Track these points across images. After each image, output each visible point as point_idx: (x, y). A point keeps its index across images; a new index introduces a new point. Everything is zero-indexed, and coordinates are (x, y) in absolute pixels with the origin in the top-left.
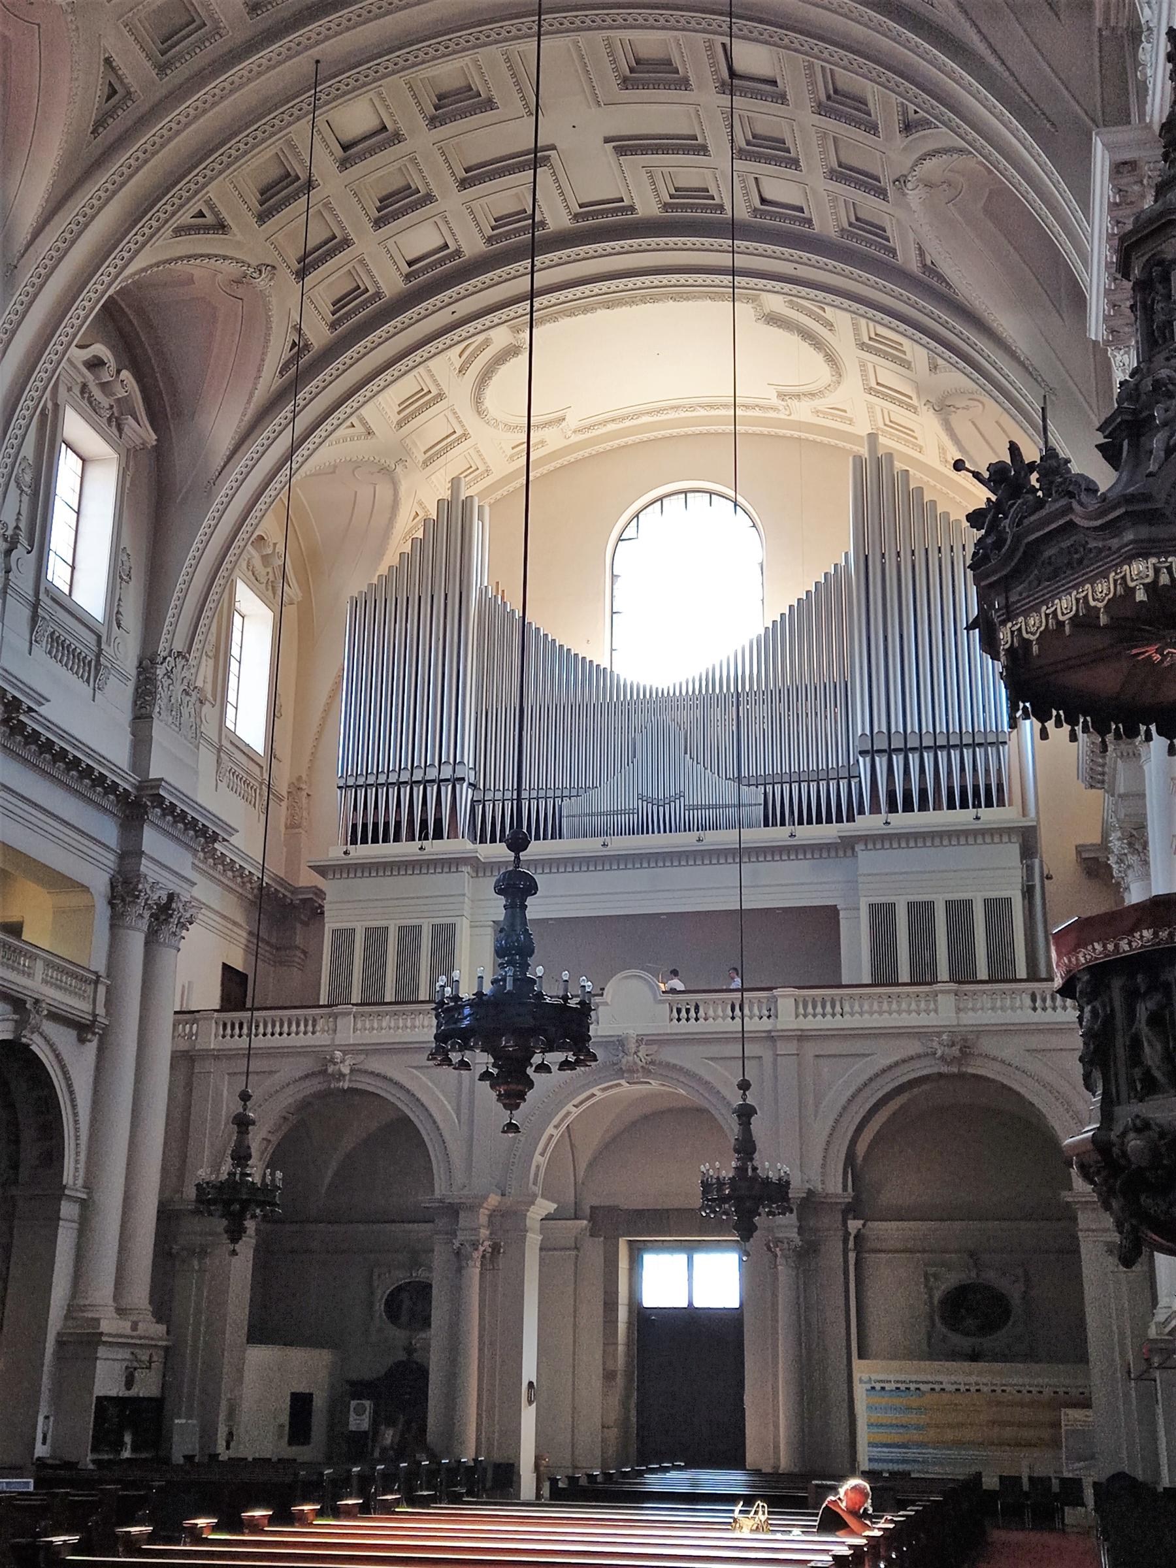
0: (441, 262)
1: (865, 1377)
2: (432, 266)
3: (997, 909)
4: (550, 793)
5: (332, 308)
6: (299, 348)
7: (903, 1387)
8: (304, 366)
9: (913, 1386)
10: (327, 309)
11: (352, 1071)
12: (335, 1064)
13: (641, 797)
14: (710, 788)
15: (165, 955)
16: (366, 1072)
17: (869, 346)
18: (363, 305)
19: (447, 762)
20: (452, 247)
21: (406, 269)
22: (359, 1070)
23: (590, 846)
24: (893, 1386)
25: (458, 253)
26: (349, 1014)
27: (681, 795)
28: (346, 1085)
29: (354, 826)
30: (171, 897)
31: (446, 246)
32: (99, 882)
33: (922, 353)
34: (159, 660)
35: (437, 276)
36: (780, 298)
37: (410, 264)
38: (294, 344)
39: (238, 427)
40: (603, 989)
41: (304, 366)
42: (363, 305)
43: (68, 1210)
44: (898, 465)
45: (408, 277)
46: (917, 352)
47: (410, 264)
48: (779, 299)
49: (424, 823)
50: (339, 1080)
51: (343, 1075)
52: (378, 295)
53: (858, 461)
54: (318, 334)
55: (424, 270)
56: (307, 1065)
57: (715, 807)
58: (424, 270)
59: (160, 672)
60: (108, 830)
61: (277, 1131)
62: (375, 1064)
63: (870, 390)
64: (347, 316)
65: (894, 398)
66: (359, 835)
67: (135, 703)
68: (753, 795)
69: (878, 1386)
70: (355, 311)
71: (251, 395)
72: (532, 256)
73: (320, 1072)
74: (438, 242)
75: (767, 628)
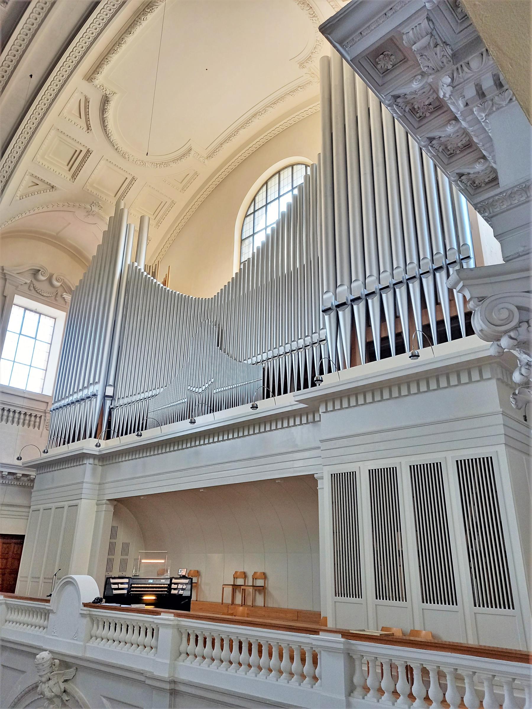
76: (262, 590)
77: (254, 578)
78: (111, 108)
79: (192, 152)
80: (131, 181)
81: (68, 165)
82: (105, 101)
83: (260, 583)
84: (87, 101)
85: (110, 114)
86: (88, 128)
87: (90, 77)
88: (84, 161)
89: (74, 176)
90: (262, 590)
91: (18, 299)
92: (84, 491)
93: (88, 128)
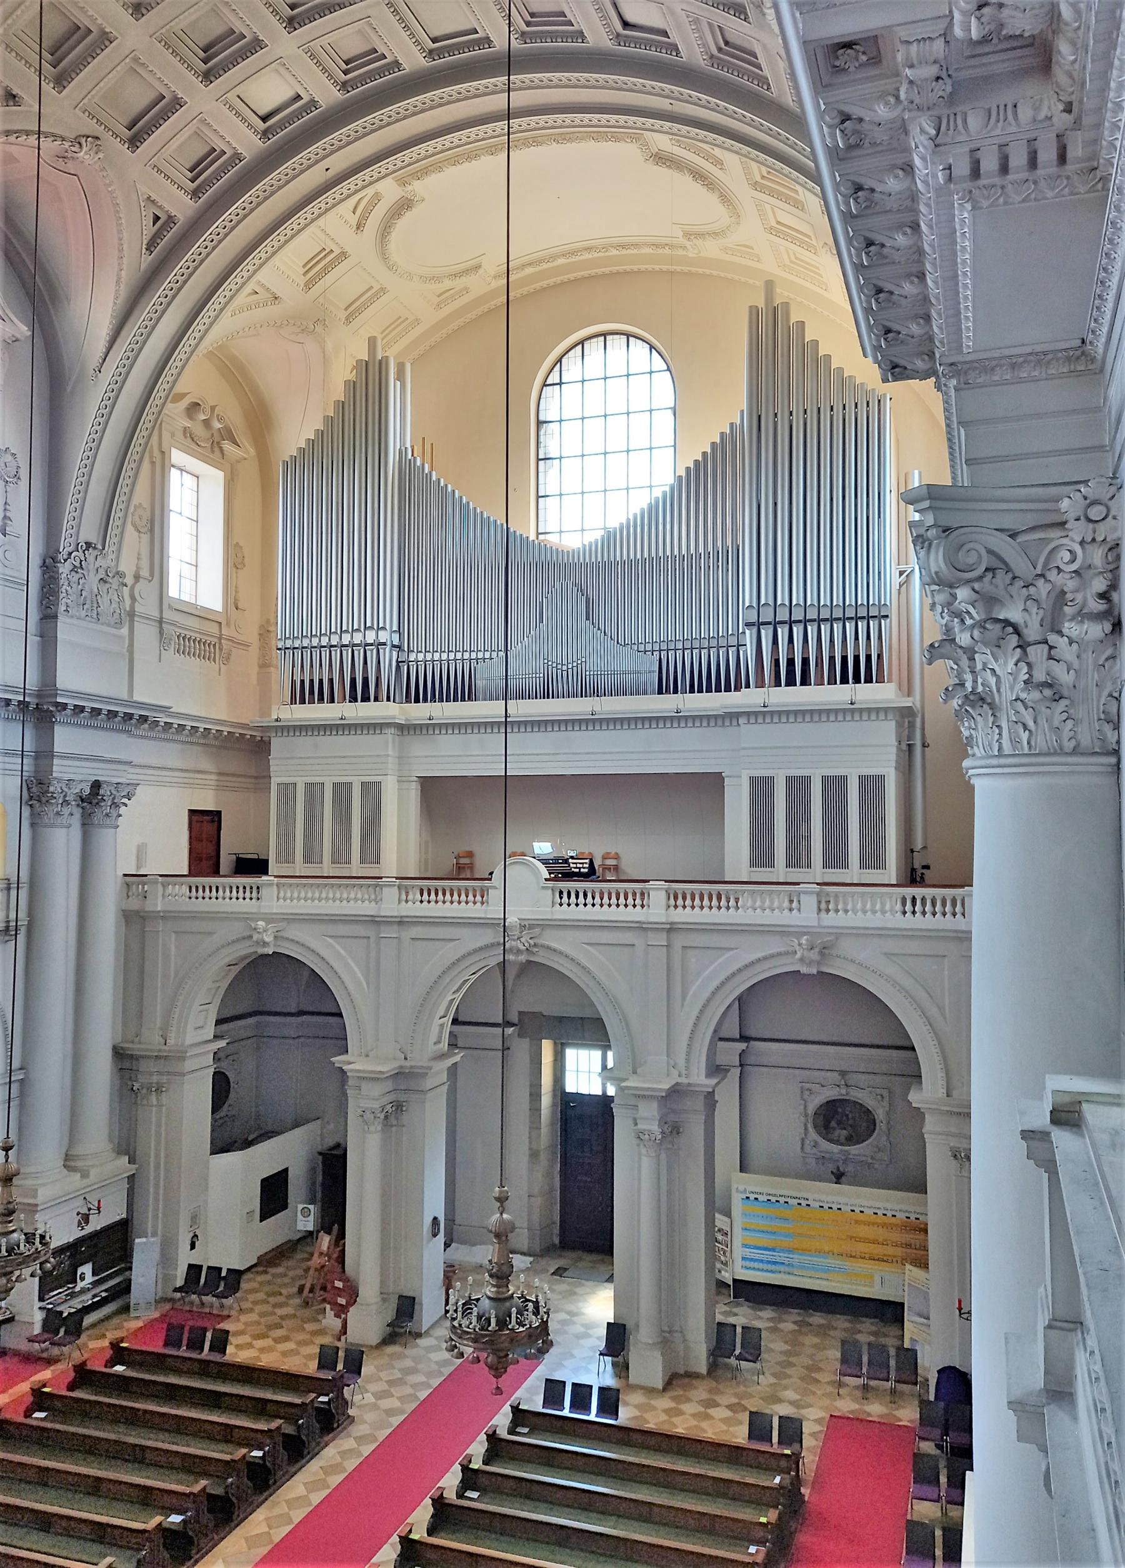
0: (297, 115)
1: (741, 1188)
2: (289, 120)
3: (872, 786)
5: (190, 175)
6: (162, 222)
7: (773, 1199)
8: (169, 243)
9: (782, 1200)
11: (275, 937)
15: (104, 836)
16: (287, 939)
17: (763, 186)
18: (224, 170)
22: (282, 937)
24: (765, 1198)
25: (313, 103)
26: (272, 884)
30: (96, 785)
31: (298, 97)
34: (60, 557)
35: (294, 132)
36: (666, 137)
37: (264, 119)
38: (157, 218)
39: (113, 311)
40: (491, 874)
41: (169, 243)
42: (224, 170)
44: (794, 318)
45: (265, 134)
47: (264, 119)
48: (665, 138)
52: (237, 157)
53: (754, 312)
55: (281, 125)
58: (281, 125)
61: (224, 978)
62: (293, 932)
63: (771, 230)
64: (208, 183)
65: (794, 238)
69: (752, 1196)
74: (289, 94)
75: (680, 477)
76: (616, 868)
77: (604, 858)
78: (408, 216)
79: (481, 271)
80: (376, 293)
81: (304, 266)
82: (405, 205)
83: (610, 862)
84: (377, 197)
86: (359, 227)
88: (333, 265)
89: (308, 286)
90: (616, 868)
91: (177, 456)
92: (390, 766)
93: (359, 227)
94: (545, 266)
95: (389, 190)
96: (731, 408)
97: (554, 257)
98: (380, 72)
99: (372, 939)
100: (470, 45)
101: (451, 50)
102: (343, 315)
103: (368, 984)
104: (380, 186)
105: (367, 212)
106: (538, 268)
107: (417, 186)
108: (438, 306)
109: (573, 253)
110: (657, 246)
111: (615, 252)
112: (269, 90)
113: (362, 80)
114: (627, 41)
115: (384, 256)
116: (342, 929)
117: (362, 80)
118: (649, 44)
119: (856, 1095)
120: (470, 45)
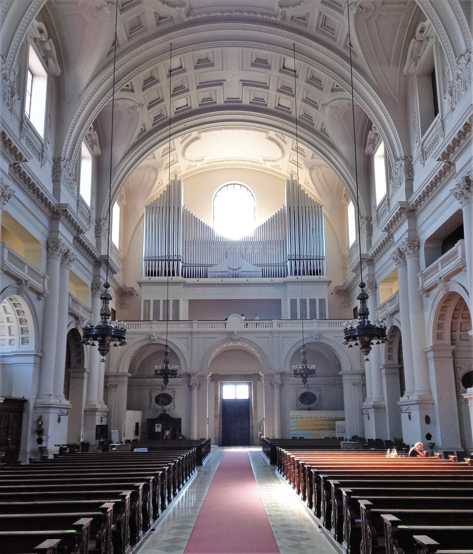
0: (185, 110)
2: (183, 111)
4: (192, 265)
6: (143, 130)
8: (145, 135)
10: (153, 119)
12: (153, 336)
13: (229, 268)
14: (247, 266)
16: (161, 339)
18: (162, 120)
19: (176, 255)
20: (189, 105)
21: (175, 111)
23: (218, 280)
25: (190, 108)
27: (240, 268)
28: (155, 342)
29: (149, 271)
31: (187, 105)
32: (89, 283)
33: (311, 152)
35: (185, 114)
37: (177, 109)
41: (145, 135)
42: (162, 120)
43: (86, 375)
46: (308, 151)
49: (169, 272)
50: (154, 341)
51: (155, 339)
54: (149, 127)
56: (144, 337)
57: (249, 272)
59: (102, 223)
60: (90, 268)
66: (150, 274)
67: (95, 232)
68: (259, 269)
70: (160, 121)
71: (129, 143)
72: (211, 111)
73: (148, 339)
78: (197, 142)
84: (190, 135)
85: (193, 144)
87: (200, 133)
94: (220, 163)
95: (194, 134)
96: (281, 202)
97: (223, 161)
98: (210, 103)
99: (189, 338)
100: (236, 102)
101: (230, 102)
102: (165, 166)
103: (188, 351)
104: (193, 133)
105: (186, 138)
106: (218, 163)
107: (203, 135)
108: (187, 169)
109: (229, 161)
110: (253, 162)
111: (241, 162)
112: (181, 102)
113: (205, 104)
114: (278, 108)
115: (184, 152)
116: (179, 336)
117: (205, 104)
118: (283, 110)
119: (312, 391)
120: (236, 102)
